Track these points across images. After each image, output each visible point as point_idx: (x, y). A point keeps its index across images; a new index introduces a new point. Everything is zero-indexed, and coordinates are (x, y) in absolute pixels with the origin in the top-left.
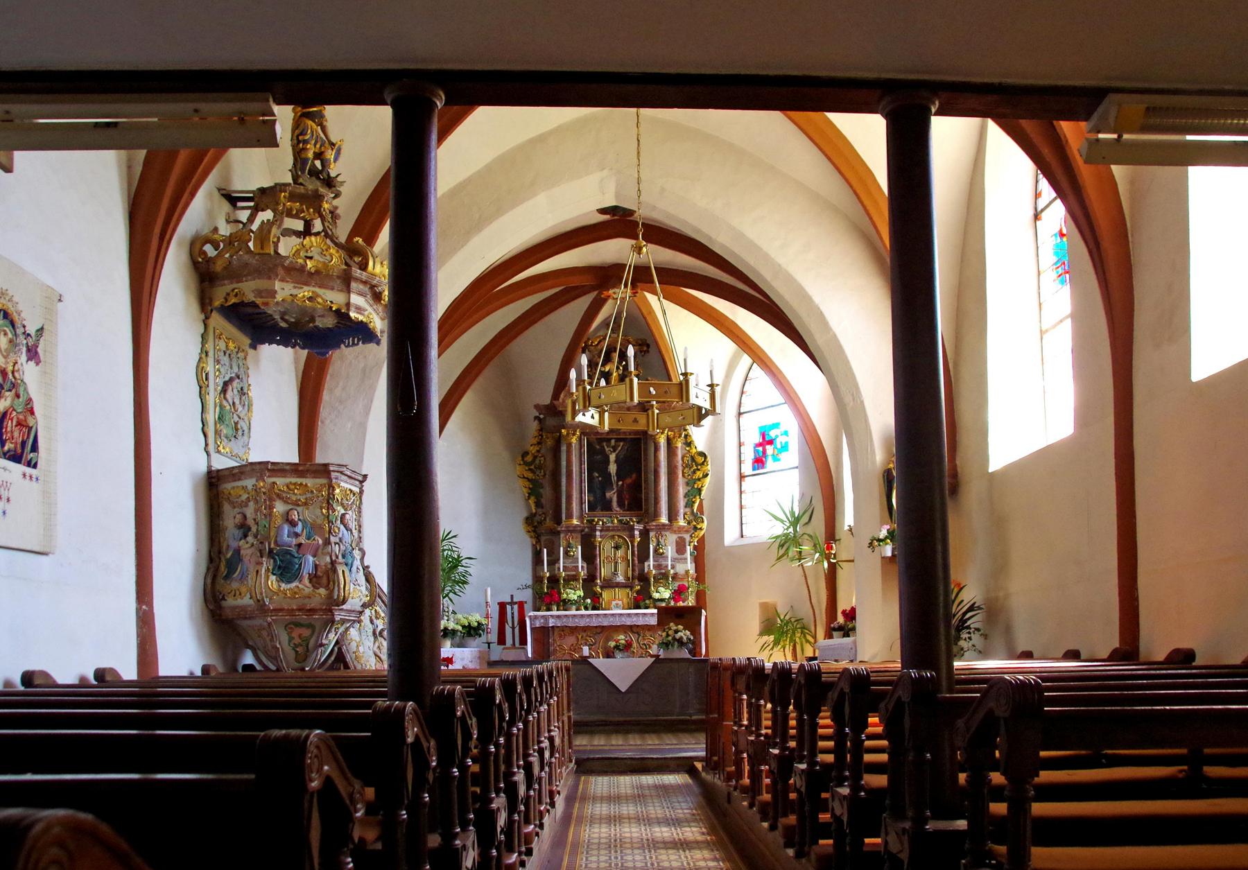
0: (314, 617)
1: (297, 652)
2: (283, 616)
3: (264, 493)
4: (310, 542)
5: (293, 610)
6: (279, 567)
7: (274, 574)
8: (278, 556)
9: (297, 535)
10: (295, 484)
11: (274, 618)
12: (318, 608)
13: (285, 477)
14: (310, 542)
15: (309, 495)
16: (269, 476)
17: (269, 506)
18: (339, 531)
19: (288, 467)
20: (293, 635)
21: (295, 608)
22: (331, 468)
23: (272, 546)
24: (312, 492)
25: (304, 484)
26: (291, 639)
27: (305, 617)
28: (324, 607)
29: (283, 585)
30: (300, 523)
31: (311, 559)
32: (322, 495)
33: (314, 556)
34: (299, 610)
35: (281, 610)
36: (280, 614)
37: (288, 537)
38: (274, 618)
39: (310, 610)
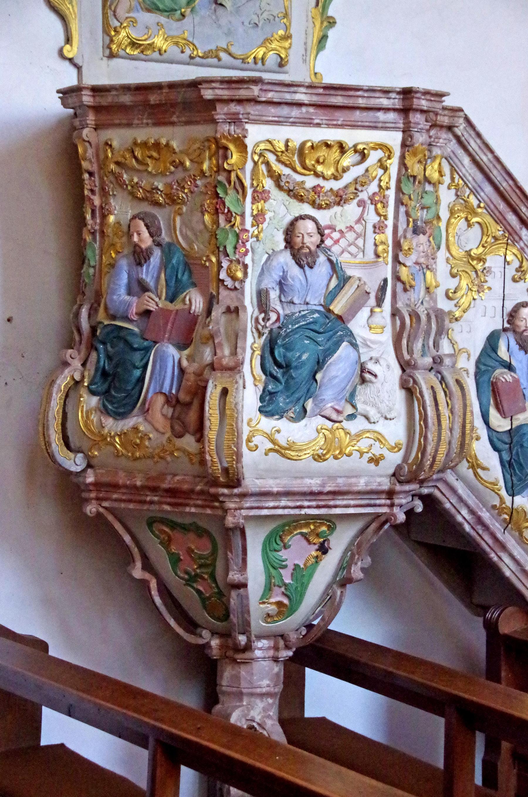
0: (187, 509)
1: (198, 591)
2: (116, 500)
3: (91, 174)
4: (171, 306)
5: (135, 487)
6: (105, 374)
7: (93, 393)
8: (104, 343)
9: (144, 288)
10: (145, 145)
11: (106, 504)
12: (185, 487)
13: (129, 125)
14: (171, 306)
15: (180, 175)
16: (96, 128)
17: (102, 208)
18: (246, 274)
19: (126, 99)
20: (173, 549)
21: (139, 483)
22: (208, 94)
23: (101, 316)
24: (182, 164)
25: (164, 141)
26: (175, 560)
27: (167, 508)
28: (199, 488)
29: (109, 423)
30: (157, 255)
31: (171, 351)
32: (203, 174)
33: (182, 346)
34: (154, 490)
35: (115, 486)
36: (115, 496)
37: (129, 293)
38: (106, 504)
39: (172, 492)
